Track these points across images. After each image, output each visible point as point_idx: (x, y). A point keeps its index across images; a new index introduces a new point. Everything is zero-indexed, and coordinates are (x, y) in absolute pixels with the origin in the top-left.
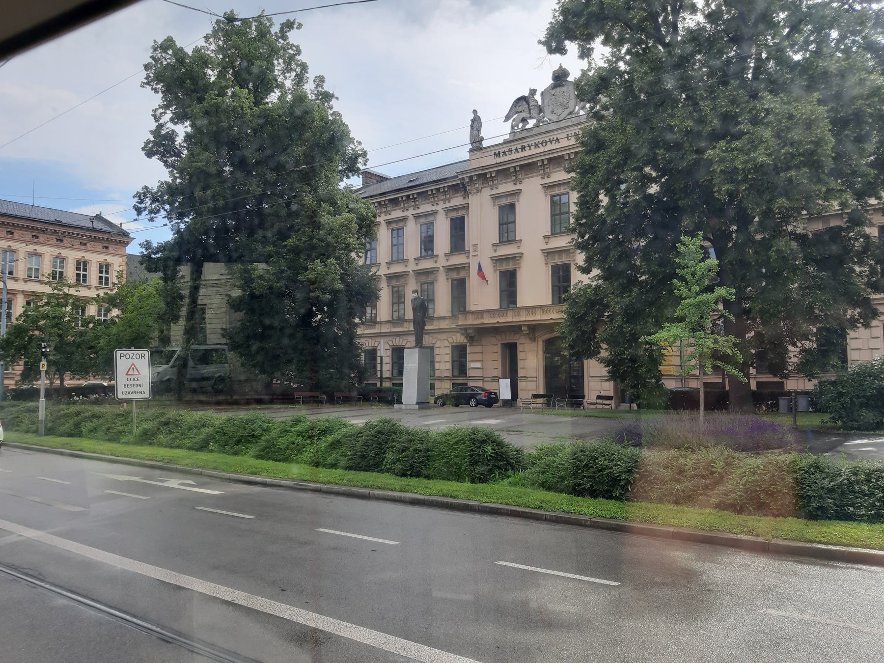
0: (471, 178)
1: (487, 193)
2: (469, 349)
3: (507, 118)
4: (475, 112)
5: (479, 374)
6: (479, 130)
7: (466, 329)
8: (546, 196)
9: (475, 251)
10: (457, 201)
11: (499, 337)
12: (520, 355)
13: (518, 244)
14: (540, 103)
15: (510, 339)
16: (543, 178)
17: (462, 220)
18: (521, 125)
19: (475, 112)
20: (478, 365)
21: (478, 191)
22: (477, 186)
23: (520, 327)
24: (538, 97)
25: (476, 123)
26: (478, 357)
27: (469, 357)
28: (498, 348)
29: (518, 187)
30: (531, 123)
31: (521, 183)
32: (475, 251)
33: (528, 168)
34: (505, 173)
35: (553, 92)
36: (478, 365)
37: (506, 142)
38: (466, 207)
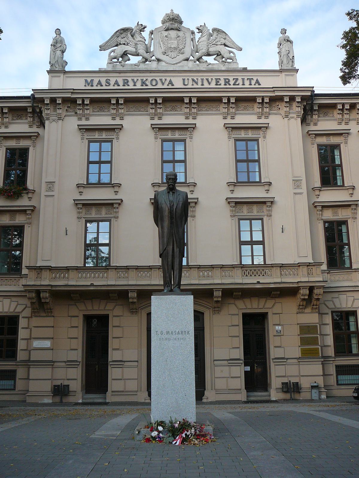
0: (53, 100)
1: (72, 123)
2: (22, 323)
3: (102, 48)
4: (58, 31)
5: (47, 356)
6: (63, 52)
7: (38, 292)
8: (156, 138)
9: (50, 189)
10: (20, 127)
11: (82, 306)
12: (113, 332)
13: (116, 189)
14: (147, 43)
15: (97, 308)
16: (152, 119)
17: (24, 153)
18: (120, 59)
19: (58, 31)
20: (47, 344)
21: (60, 119)
22: (59, 111)
23: (126, 292)
24: (146, 34)
25: (58, 45)
26: (49, 332)
27: (22, 334)
28: (79, 322)
29: (118, 122)
30: (134, 60)
31: (122, 119)
32: (50, 189)
33: (137, 102)
34: (101, 102)
35: (166, 33)
36: (47, 344)
37: (100, 72)
38: (34, 137)
